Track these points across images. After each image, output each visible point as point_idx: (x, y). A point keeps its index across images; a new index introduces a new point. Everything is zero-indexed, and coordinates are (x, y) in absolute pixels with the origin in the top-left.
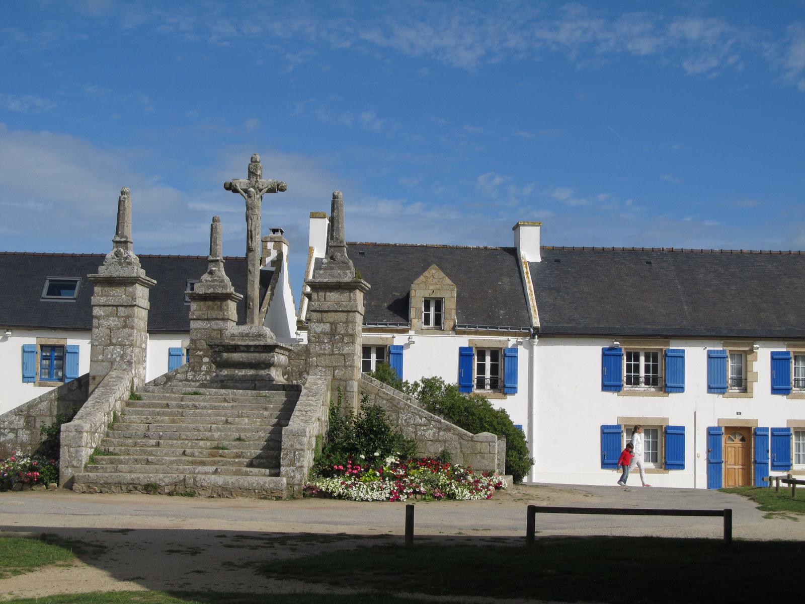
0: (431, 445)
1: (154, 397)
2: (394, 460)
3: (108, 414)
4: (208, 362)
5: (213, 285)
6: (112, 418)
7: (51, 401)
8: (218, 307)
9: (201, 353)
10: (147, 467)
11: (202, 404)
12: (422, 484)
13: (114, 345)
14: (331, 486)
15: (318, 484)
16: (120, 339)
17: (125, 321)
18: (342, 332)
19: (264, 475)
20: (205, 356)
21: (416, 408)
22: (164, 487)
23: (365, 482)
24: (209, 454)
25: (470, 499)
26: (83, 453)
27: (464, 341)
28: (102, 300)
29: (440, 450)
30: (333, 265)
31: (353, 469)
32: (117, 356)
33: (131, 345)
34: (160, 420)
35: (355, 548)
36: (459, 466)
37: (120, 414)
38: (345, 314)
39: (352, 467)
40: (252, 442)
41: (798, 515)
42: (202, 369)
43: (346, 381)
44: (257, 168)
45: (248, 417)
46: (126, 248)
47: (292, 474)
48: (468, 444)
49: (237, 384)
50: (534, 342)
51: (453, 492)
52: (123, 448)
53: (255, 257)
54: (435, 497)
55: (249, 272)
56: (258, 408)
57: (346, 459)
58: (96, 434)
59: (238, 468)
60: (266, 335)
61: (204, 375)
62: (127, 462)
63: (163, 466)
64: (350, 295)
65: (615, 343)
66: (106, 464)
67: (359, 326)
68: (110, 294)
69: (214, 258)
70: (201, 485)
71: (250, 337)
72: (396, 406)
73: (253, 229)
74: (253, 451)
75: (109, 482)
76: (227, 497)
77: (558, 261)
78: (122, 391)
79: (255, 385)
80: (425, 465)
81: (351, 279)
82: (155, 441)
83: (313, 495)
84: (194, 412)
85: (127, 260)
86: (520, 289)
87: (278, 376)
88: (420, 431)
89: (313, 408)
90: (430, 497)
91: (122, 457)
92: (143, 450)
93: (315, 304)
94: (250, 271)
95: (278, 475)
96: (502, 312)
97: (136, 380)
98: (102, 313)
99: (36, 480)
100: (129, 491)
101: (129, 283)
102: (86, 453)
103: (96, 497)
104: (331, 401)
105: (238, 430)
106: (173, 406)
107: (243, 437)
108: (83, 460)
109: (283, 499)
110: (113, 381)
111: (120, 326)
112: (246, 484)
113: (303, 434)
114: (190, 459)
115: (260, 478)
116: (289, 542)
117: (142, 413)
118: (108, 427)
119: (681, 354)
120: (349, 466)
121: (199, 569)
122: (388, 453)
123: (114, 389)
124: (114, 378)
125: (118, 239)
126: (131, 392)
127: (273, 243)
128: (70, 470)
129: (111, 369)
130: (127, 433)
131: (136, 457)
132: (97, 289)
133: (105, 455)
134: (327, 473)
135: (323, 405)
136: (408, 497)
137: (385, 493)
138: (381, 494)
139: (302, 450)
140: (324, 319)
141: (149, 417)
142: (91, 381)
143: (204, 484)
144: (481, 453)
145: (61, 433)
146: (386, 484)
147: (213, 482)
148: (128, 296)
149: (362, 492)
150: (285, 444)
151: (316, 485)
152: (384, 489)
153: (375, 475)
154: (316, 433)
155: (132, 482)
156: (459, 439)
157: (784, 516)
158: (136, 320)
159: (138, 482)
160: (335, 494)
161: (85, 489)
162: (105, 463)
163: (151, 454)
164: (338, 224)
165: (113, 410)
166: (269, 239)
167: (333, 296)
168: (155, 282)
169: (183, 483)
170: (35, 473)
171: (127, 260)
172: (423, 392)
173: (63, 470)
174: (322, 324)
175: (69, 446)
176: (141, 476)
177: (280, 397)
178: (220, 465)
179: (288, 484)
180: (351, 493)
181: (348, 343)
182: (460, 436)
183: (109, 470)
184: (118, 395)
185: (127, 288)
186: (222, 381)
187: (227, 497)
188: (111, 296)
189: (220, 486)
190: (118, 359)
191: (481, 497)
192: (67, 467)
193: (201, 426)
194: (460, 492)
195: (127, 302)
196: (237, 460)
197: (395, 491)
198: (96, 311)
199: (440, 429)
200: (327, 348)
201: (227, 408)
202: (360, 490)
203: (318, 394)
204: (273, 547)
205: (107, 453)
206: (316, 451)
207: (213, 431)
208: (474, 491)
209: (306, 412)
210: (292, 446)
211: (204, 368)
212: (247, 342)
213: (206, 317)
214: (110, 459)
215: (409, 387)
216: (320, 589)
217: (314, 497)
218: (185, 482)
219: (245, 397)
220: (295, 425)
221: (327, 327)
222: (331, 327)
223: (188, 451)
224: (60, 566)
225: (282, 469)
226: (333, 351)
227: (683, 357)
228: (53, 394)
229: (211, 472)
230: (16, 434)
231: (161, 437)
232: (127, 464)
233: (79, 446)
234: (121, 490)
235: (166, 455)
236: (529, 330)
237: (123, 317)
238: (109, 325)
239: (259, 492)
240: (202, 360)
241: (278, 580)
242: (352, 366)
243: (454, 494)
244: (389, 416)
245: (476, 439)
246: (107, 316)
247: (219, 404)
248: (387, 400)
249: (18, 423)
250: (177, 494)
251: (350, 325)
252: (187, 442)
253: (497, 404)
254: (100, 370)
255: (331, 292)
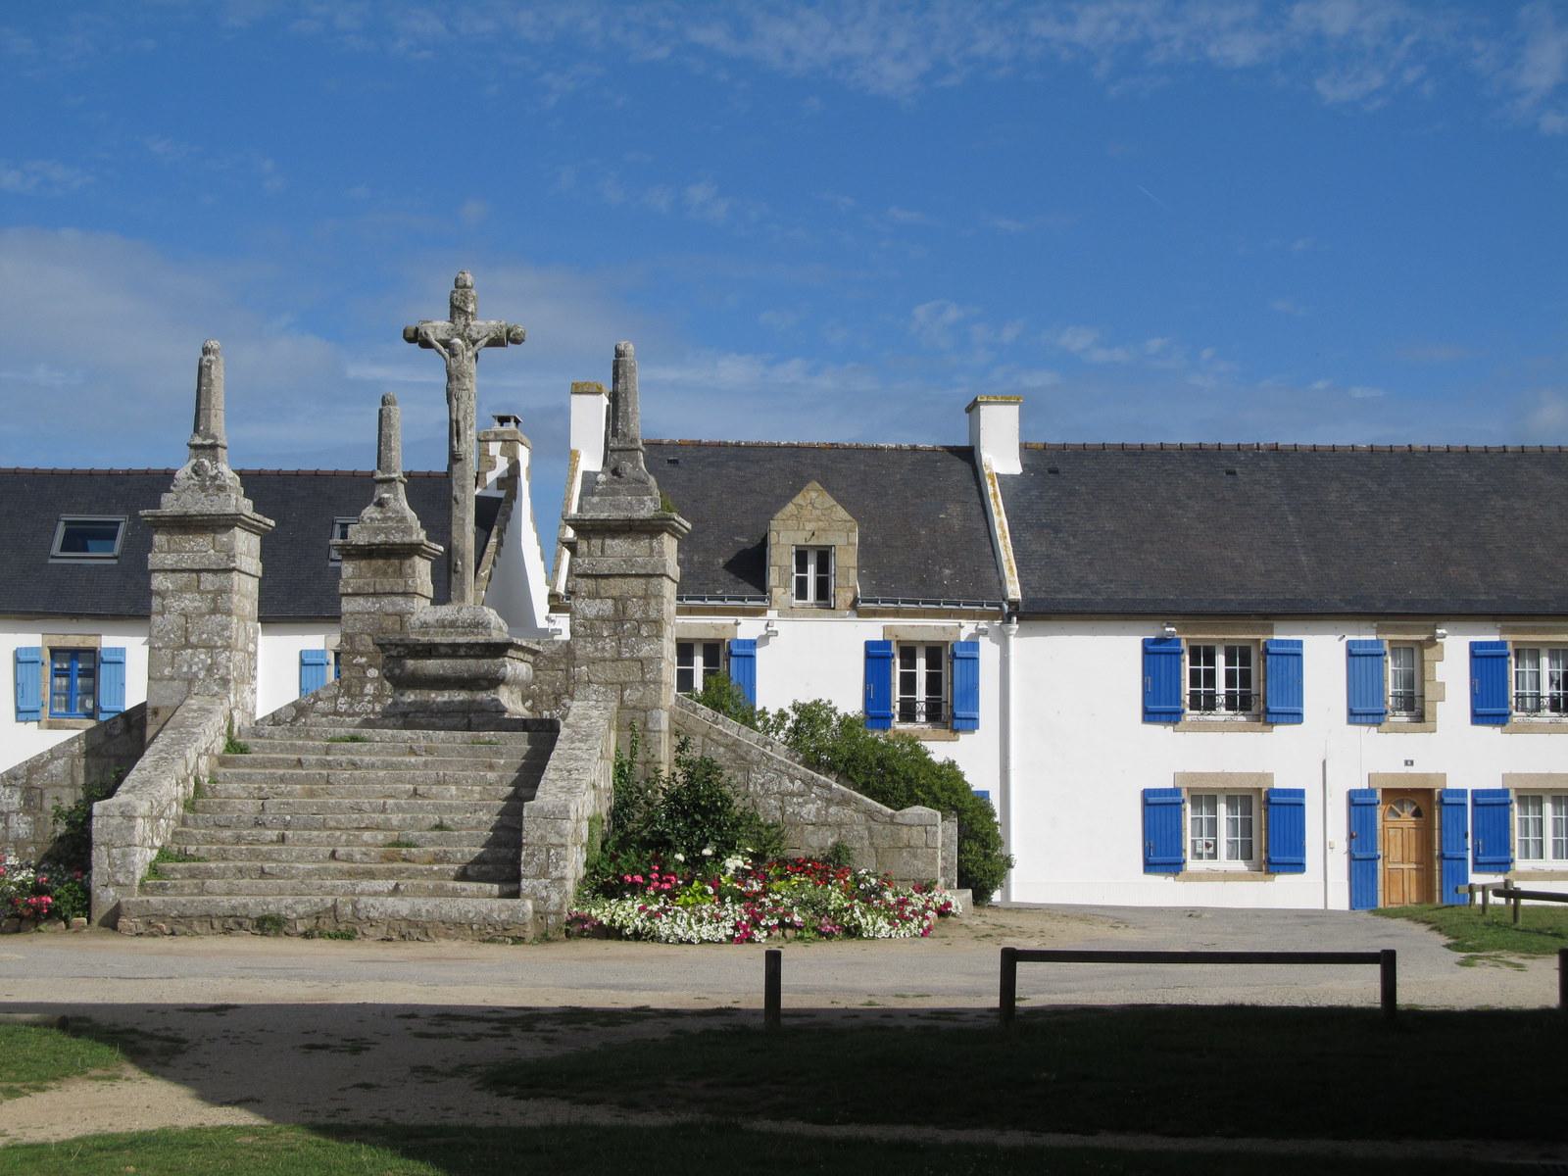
0: (813, 833)
1: (273, 748)
2: (740, 864)
3: (185, 780)
4: (378, 678)
5: (386, 528)
6: (192, 789)
7: (73, 757)
8: (395, 572)
9: (364, 660)
10: (262, 883)
11: (367, 759)
12: (795, 909)
13: (195, 647)
14: (619, 915)
15: (593, 912)
16: (205, 636)
17: (214, 600)
18: (637, 616)
19: (490, 896)
20: (370, 666)
21: (783, 762)
22: (294, 921)
23: (685, 906)
24: (381, 857)
25: (890, 936)
26: (137, 858)
27: (874, 629)
28: (170, 560)
29: (830, 841)
30: (617, 486)
31: (661, 882)
32: (200, 669)
33: (227, 647)
34: (285, 792)
35: (668, 1035)
36: (868, 873)
37: (206, 780)
38: (642, 581)
39: (661, 877)
40: (464, 833)
41: (1525, 958)
42: (366, 691)
43: (645, 711)
44: (467, 298)
45: (457, 783)
46: (215, 459)
47: (544, 894)
48: (884, 828)
49: (433, 720)
50: (1011, 629)
51: (857, 923)
52: (215, 847)
53: (465, 471)
54: (822, 934)
55: (454, 502)
56: (475, 766)
57: (648, 862)
58: (162, 821)
59: (438, 882)
60: (489, 623)
61: (369, 702)
62: (222, 875)
63: (293, 881)
64: (651, 544)
65: (1168, 629)
66: (182, 878)
67: (670, 603)
68: (185, 547)
69: (387, 475)
70: (368, 917)
71: (458, 627)
72: (743, 759)
73: (460, 418)
74: (466, 849)
75: (188, 913)
76: (418, 939)
77: (1054, 471)
78: (211, 737)
79: (470, 721)
80: (801, 873)
81: (652, 514)
82: (277, 832)
83: (585, 934)
84: (351, 775)
85: (217, 482)
86: (982, 525)
87: (513, 702)
88: (790, 806)
89: (582, 763)
90: (812, 934)
91: (212, 865)
92: (254, 849)
93: (584, 561)
94: (456, 499)
95: (516, 894)
96: (947, 571)
97: (237, 714)
98: (169, 585)
99: (45, 911)
100: (228, 931)
101: (221, 527)
102: (143, 858)
103: (163, 943)
104: (618, 750)
105: (437, 808)
106: (310, 765)
107: (447, 822)
108: (137, 871)
109: (527, 941)
110: (193, 718)
111: (204, 609)
112: (454, 914)
113: (564, 815)
114: (346, 866)
115: (482, 901)
116: (539, 1026)
117: (249, 779)
118: (185, 806)
119: (1295, 650)
120: (654, 876)
121: (367, 1081)
122: (729, 849)
123: (194, 733)
124: (195, 711)
125: (198, 441)
126: (229, 738)
127: (501, 443)
128: (111, 891)
129: (188, 694)
130: (222, 818)
131: (240, 864)
132: (159, 539)
133: (180, 862)
134: (611, 890)
135: (601, 758)
136: (769, 935)
137: (724, 927)
138: (716, 929)
139: (562, 845)
140: (602, 591)
141: (264, 786)
142: (149, 718)
143: (373, 914)
144: (909, 846)
145: (94, 820)
146: (727, 910)
147: (390, 911)
148: (221, 551)
149: (679, 926)
150: (528, 834)
151: (590, 914)
152: (722, 919)
153: (704, 892)
154: (588, 812)
155: (232, 913)
156: (867, 821)
157: (1498, 962)
158: (236, 598)
159: (244, 913)
160: (628, 931)
161: (142, 928)
162: (179, 876)
163: (268, 857)
164: (627, 406)
165: (194, 774)
166: (492, 436)
167: (618, 546)
168: (272, 523)
169: (332, 914)
170: (44, 898)
171: (217, 482)
172: (796, 731)
173: (98, 891)
174: (598, 601)
175: (109, 845)
176: (251, 901)
177: (518, 744)
178: (403, 878)
179: (536, 912)
180: (658, 928)
181: (649, 636)
182: (870, 815)
183: (187, 890)
184: (202, 744)
185: (218, 536)
186: (405, 715)
187: (418, 939)
188: (186, 552)
189: (404, 919)
190: (202, 675)
191: (911, 932)
192: (106, 886)
193: (365, 803)
194: (870, 922)
195: (219, 564)
196: (436, 868)
197: (744, 923)
198: (158, 582)
199: (829, 802)
200: (608, 647)
201: (415, 767)
202: (675, 923)
203: (591, 736)
204: (509, 1035)
205: (183, 857)
206: (589, 846)
207: (389, 811)
208: (897, 921)
209: (569, 771)
210: (542, 838)
211: (369, 689)
212: (453, 638)
213: (372, 591)
214: (189, 869)
215: (769, 720)
216: (602, 1116)
217: (588, 937)
218: (335, 911)
219: (449, 745)
220: (549, 798)
221: (607, 607)
222: (615, 605)
223: (341, 851)
224: (96, 1079)
225: (525, 883)
226: (619, 653)
227: (1299, 655)
228: (77, 744)
229: (386, 891)
230: (6, 824)
231: (287, 826)
232: (223, 878)
233: (129, 845)
234: (212, 928)
235: (299, 858)
236: (1001, 606)
237: (209, 592)
238: (183, 609)
239: (480, 929)
240: (364, 672)
241: (520, 1098)
242: (658, 683)
243: (858, 927)
244: (730, 778)
245: (899, 819)
246: (180, 591)
247: (400, 759)
248: (726, 746)
249: (10, 800)
250: (321, 935)
251: (653, 602)
252: (338, 833)
253: (939, 750)
254: (168, 695)
255: (613, 538)
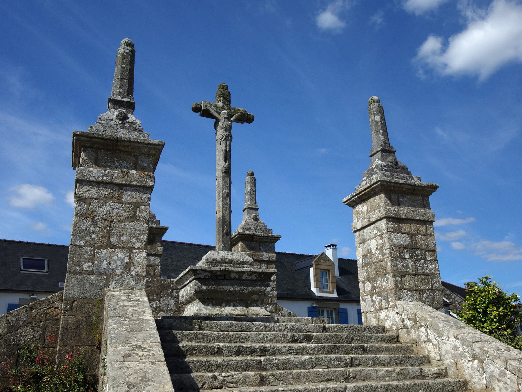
13: (114, 247)
16: (124, 238)
171: (134, 126)
200: (410, 265)
227: (347, 313)
246: (102, 200)
